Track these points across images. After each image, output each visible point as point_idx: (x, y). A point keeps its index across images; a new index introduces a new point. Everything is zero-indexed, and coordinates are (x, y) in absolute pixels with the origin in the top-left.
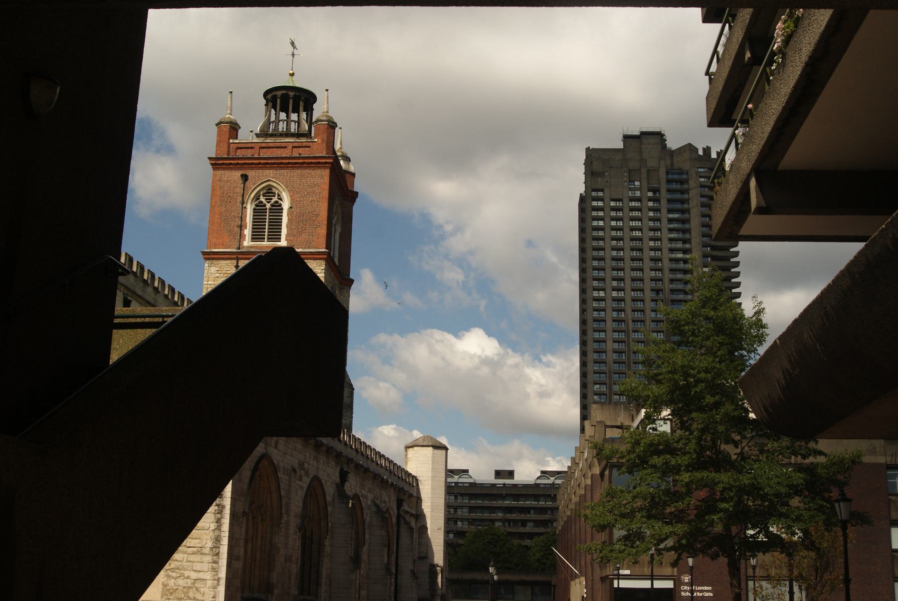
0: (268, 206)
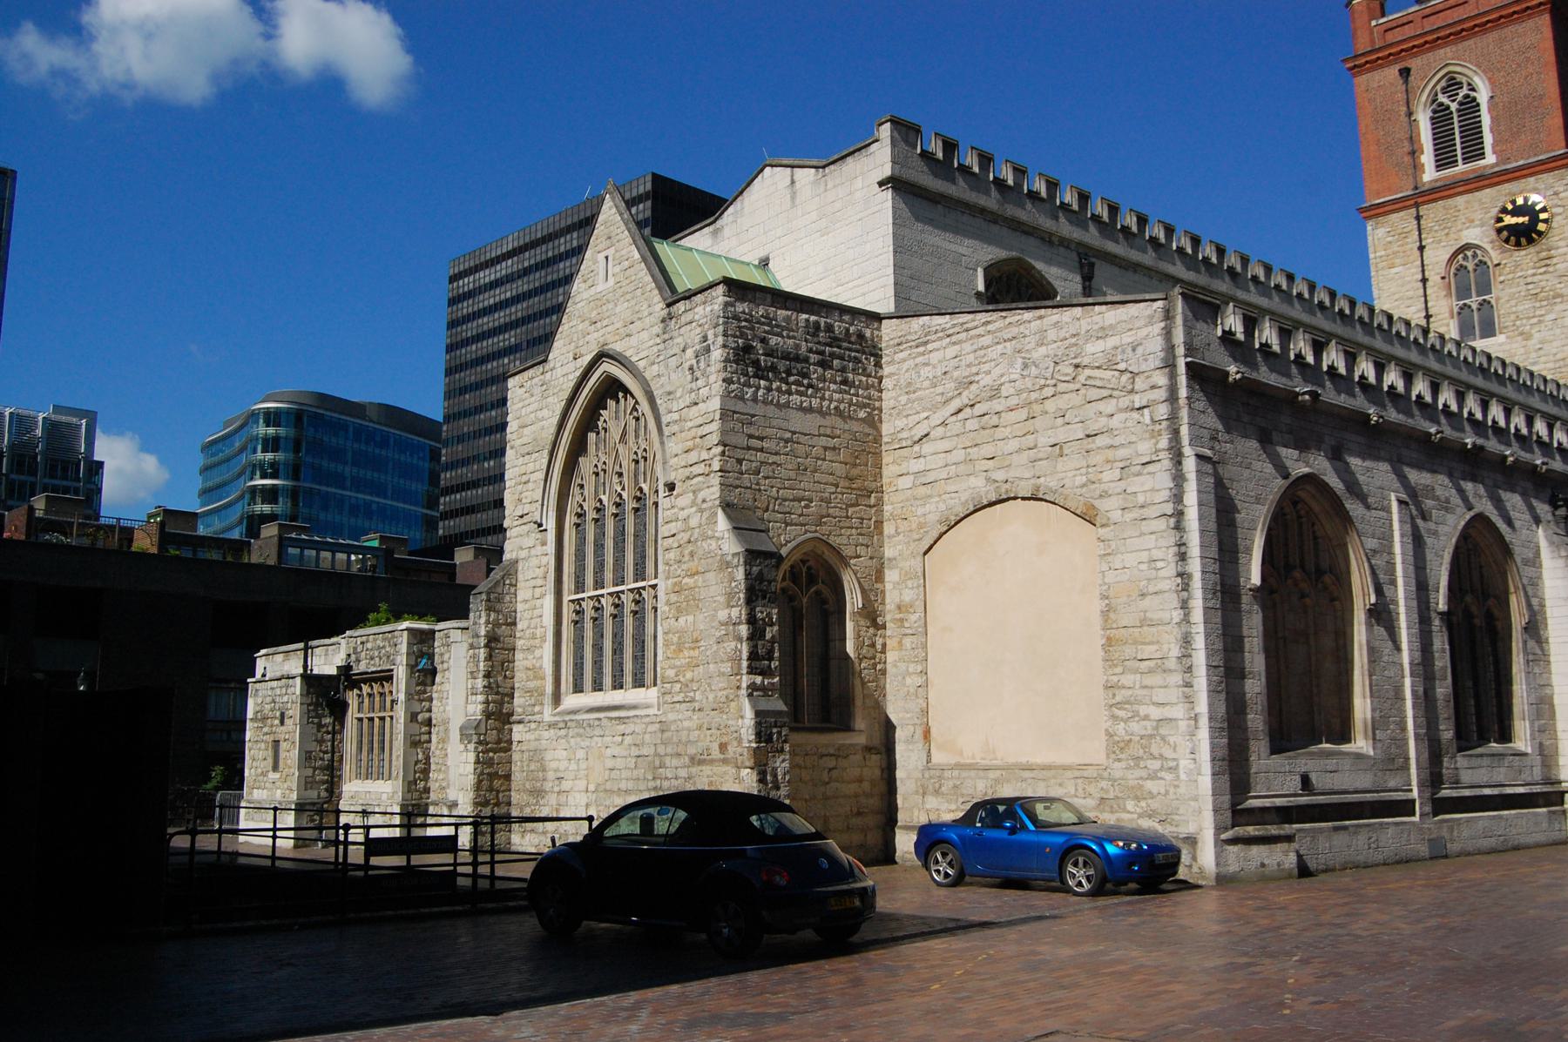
0: (1454, 107)
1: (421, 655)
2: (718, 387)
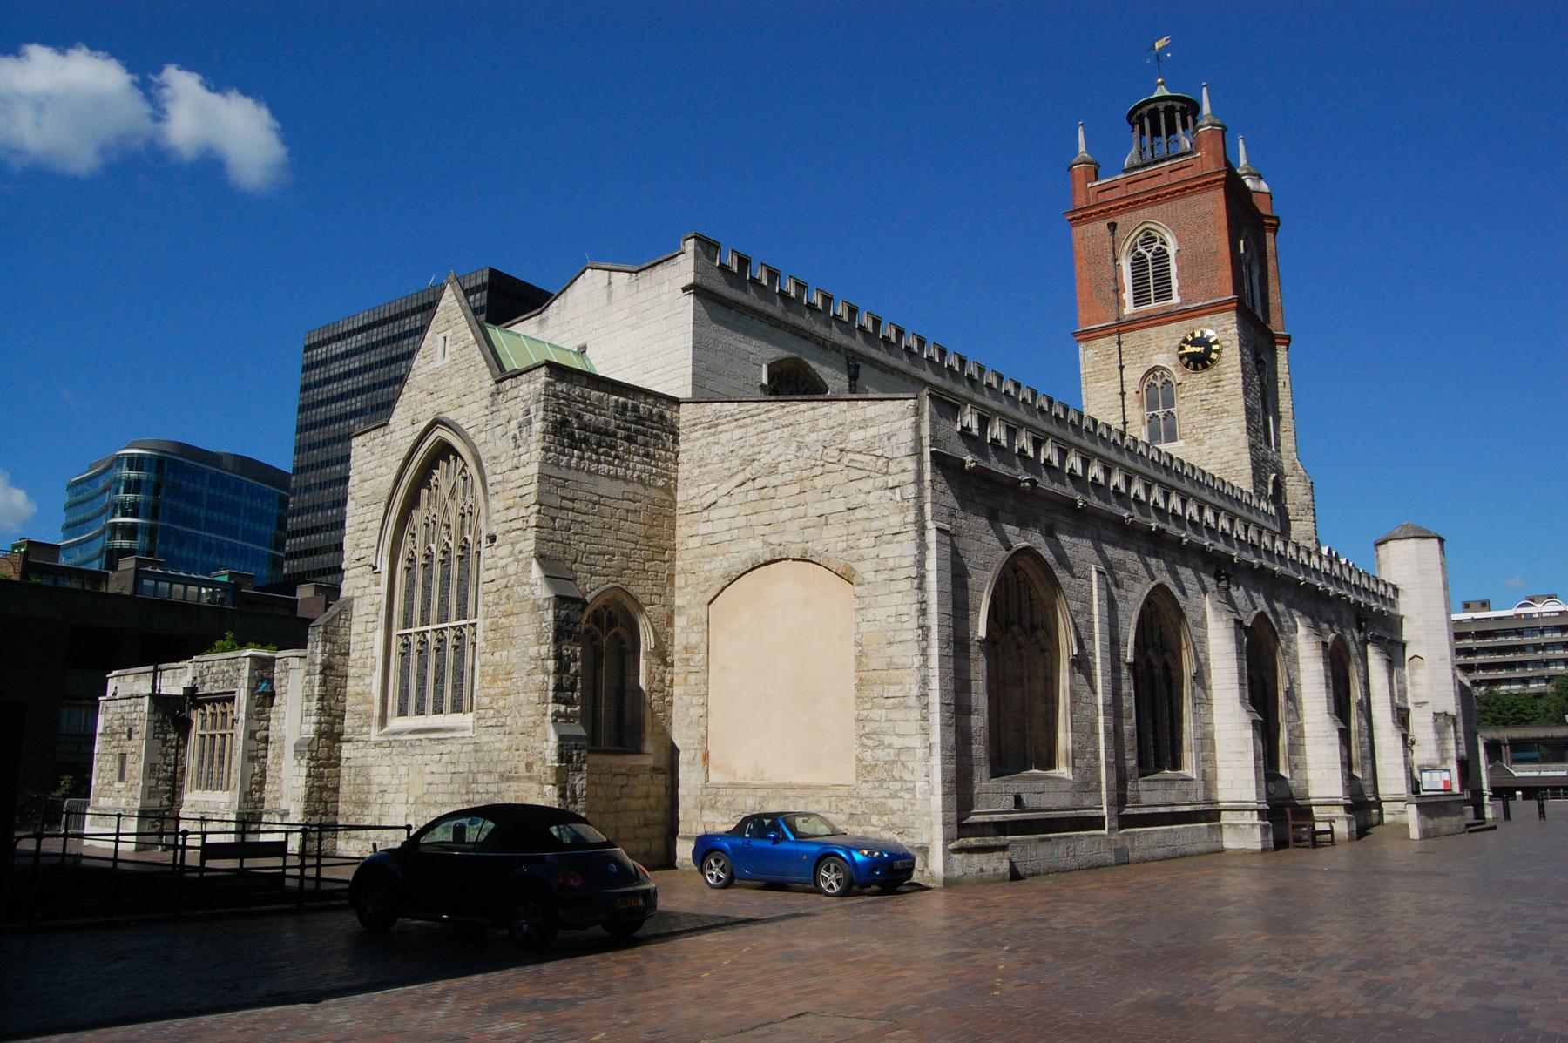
0: (1149, 256)
1: (262, 679)
2: (537, 454)
